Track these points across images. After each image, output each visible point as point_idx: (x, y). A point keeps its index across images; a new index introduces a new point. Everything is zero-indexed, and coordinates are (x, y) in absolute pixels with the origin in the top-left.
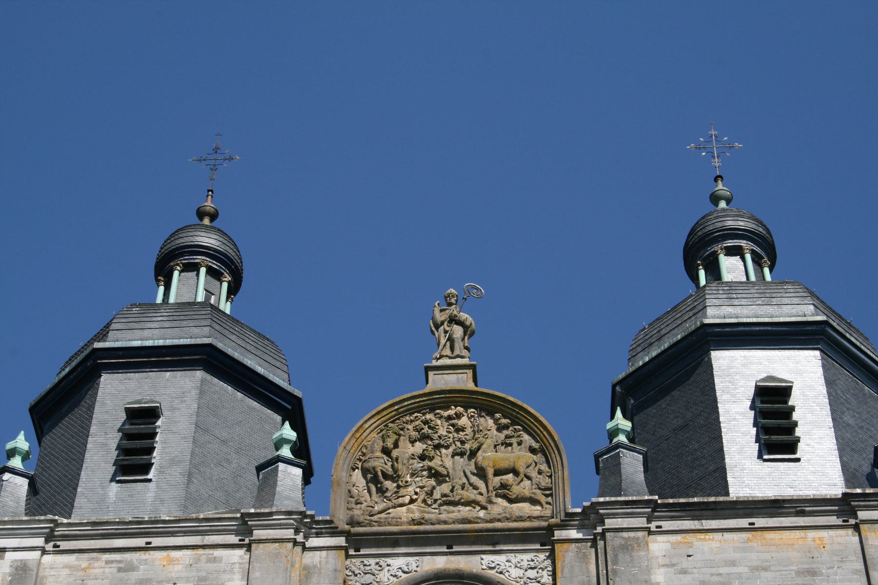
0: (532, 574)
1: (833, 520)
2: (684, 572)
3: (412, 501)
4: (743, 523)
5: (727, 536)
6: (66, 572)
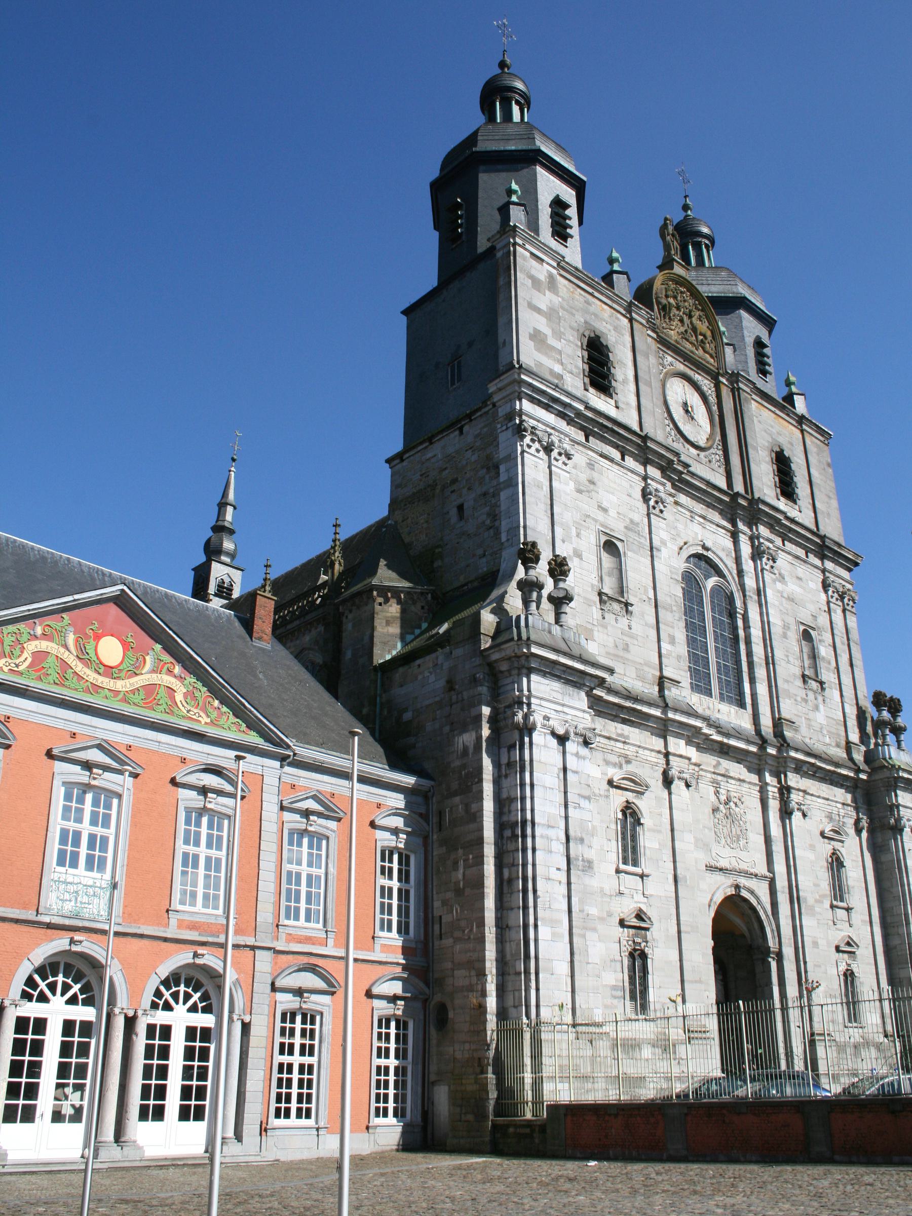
1: (794, 423)
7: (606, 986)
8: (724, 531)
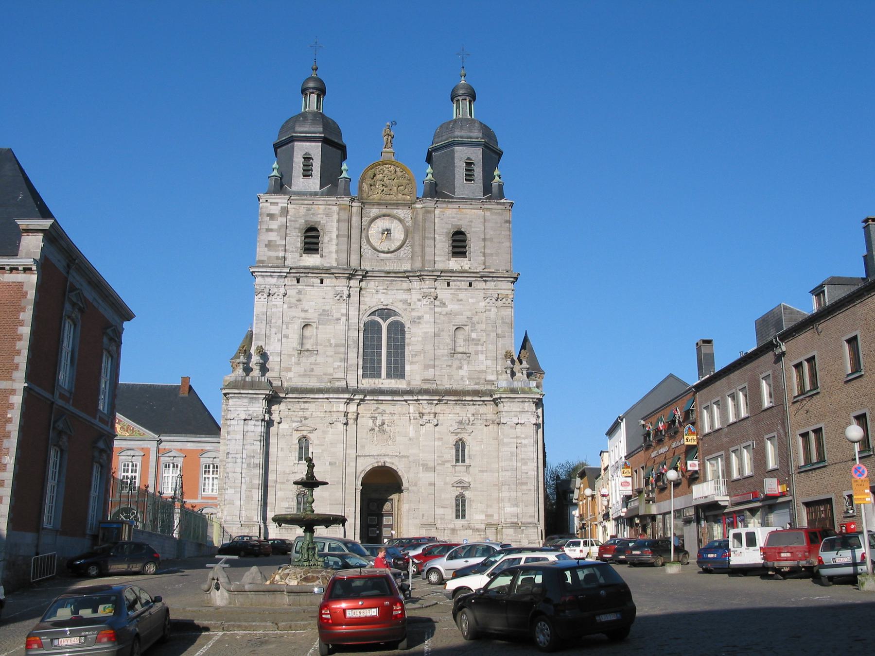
0: (406, 216)
2: (442, 219)
3: (378, 193)
5: (453, 210)
6: (294, 210)
7: (283, 507)
8: (402, 291)
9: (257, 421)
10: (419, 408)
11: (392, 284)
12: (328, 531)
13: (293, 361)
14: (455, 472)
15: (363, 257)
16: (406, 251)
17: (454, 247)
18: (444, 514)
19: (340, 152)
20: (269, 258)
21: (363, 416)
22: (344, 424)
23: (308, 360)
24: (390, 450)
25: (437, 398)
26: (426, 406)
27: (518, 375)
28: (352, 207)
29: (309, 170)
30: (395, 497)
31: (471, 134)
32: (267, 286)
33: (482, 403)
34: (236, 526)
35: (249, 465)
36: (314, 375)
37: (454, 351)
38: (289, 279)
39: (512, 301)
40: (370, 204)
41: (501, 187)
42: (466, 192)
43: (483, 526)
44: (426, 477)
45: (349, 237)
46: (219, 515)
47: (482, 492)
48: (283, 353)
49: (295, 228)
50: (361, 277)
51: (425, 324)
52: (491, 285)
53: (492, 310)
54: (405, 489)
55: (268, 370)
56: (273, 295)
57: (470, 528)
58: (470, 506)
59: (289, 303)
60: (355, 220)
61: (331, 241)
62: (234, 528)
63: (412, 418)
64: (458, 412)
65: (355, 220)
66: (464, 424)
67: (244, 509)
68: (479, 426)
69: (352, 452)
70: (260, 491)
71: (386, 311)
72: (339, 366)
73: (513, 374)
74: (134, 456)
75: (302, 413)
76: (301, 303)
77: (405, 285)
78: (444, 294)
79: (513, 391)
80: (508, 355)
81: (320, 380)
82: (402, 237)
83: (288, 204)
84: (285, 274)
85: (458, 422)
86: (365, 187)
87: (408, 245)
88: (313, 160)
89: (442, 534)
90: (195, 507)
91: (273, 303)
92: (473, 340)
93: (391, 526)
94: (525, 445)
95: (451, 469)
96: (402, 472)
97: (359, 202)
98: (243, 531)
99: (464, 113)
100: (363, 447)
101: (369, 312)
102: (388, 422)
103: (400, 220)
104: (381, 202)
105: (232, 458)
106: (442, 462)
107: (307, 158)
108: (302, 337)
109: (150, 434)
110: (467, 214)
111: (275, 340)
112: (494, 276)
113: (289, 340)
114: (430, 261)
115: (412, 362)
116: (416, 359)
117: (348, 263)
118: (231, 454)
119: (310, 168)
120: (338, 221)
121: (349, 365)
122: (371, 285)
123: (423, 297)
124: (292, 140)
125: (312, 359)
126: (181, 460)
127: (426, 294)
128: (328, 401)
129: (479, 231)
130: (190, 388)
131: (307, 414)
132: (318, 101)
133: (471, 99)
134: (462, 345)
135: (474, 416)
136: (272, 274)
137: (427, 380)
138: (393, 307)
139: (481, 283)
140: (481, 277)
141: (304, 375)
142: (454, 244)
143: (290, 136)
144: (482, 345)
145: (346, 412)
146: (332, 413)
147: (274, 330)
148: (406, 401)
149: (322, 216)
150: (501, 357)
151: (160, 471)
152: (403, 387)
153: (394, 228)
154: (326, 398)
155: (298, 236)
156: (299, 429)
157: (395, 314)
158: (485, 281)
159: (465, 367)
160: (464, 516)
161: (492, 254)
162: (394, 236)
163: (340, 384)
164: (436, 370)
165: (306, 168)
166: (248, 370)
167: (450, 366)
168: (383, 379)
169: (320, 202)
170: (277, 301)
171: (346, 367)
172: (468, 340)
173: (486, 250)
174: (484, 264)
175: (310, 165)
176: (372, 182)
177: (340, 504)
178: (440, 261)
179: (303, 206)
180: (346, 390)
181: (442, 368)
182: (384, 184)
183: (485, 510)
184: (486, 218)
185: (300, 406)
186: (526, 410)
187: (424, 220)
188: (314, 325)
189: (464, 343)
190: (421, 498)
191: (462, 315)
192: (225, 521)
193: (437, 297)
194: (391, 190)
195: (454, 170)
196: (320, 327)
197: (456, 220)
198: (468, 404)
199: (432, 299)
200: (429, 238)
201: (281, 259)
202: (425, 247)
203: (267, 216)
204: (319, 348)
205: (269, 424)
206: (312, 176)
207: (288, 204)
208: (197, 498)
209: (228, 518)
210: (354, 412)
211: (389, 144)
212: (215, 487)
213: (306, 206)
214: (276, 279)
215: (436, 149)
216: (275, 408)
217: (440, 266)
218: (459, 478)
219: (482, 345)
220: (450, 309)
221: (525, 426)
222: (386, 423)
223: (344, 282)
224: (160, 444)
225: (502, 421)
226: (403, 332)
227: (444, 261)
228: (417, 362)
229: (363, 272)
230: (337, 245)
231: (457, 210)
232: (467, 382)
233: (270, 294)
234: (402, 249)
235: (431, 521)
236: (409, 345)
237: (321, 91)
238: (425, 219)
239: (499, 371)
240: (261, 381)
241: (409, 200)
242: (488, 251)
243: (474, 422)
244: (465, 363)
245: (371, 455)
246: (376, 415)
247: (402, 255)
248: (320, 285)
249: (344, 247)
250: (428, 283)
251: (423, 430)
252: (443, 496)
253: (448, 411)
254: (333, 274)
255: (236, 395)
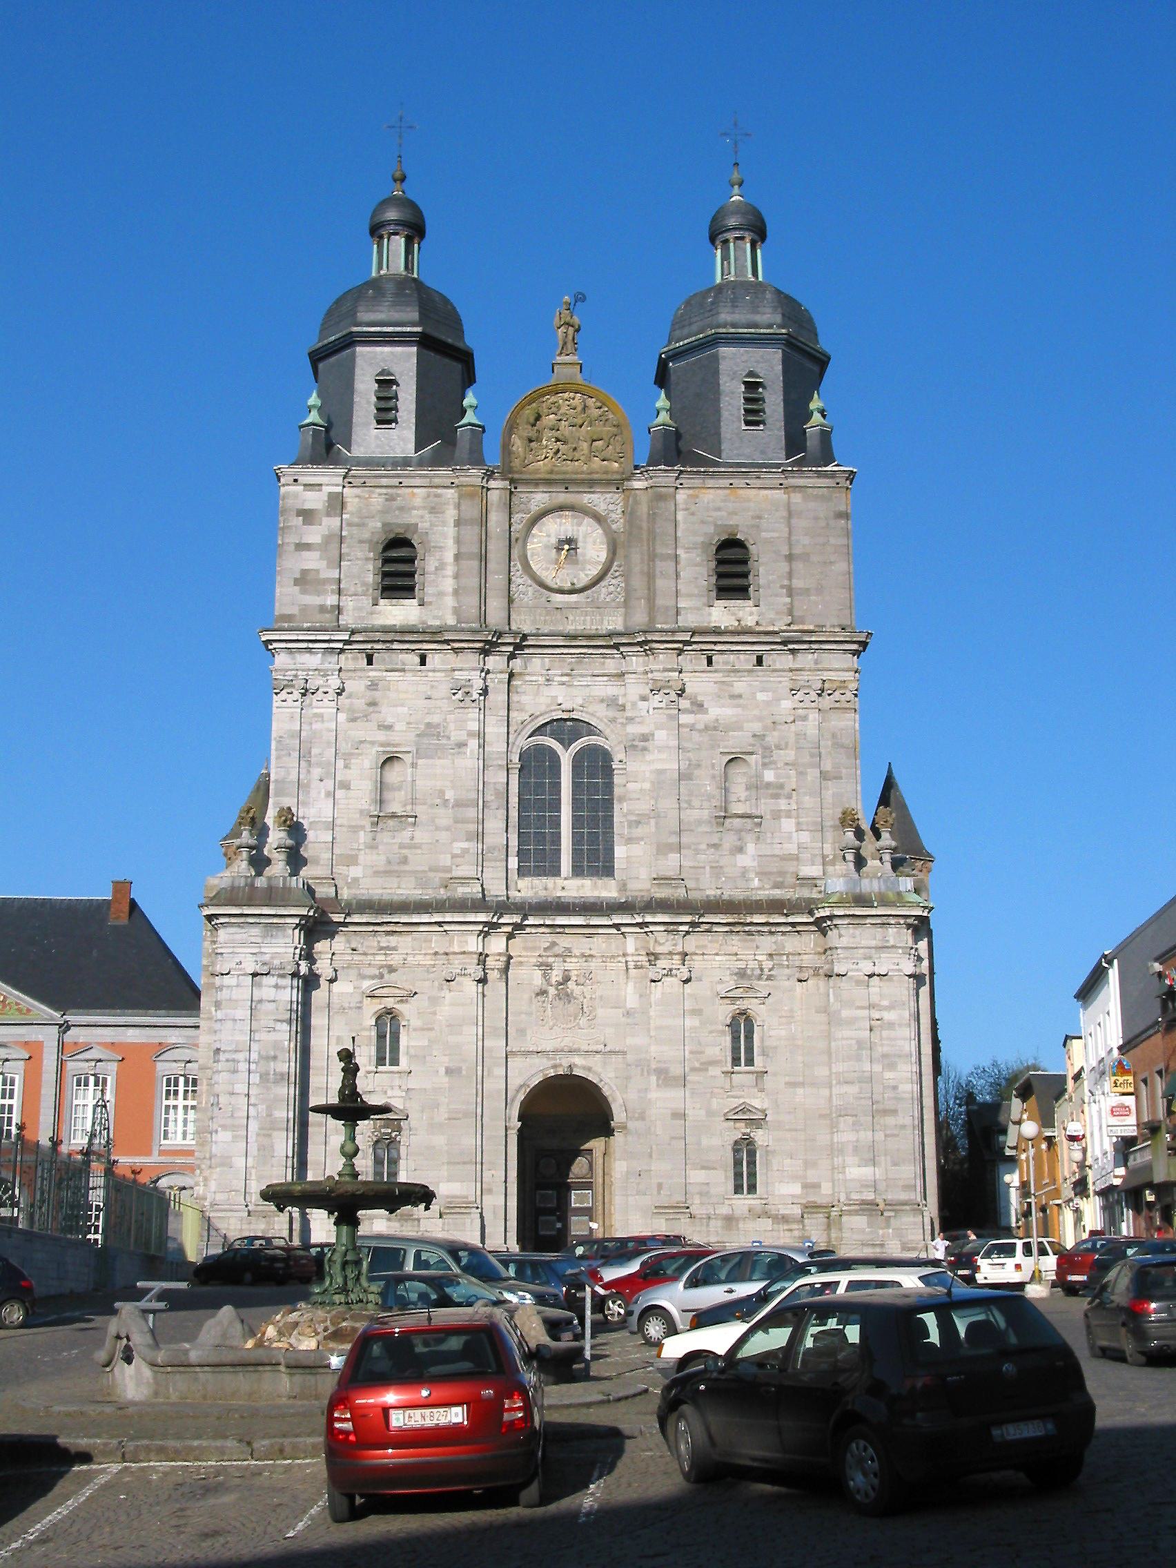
0: (611, 507)
2: (693, 514)
3: (546, 458)
4: (726, 483)
6: (357, 500)
8: (605, 678)
9: (282, 976)
10: (648, 942)
11: (581, 662)
12: (444, 1224)
13: (362, 841)
14: (732, 1087)
15: (515, 605)
16: (612, 588)
17: (720, 576)
18: (708, 1184)
19: (458, 366)
20: (304, 609)
21: (521, 963)
22: (479, 981)
23: (394, 837)
24: (582, 1038)
25: (688, 919)
26: (662, 937)
27: (872, 863)
28: (488, 489)
29: (390, 409)
30: (596, 1144)
31: (758, 318)
32: (300, 673)
33: (789, 928)
34: (236, 1214)
35: (264, 1077)
36: (409, 872)
37: (726, 812)
38: (350, 656)
39: (856, 695)
40: (527, 482)
41: (825, 436)
42: (747, 451)
43: (797, 1211)
44: (663, 1100)
45: (483, 558)
46: (200, 1190)
47: (793, 1133)
48: (338, 822)
49: (361, 542)
50: (511, 649)
51: (659, 751)
52: (806, 660)
53: (811, 717)
54: (619, 1128)
55: (304, 862)
56: (313, 693)
57: (766, 1214)
58: (767, 1164)
59: (349, 710)
60: (496, 519)
61: (443, 569)
62: (232, 1221)
63: (631, 965)
64: (735, 950)
65: (496, 519)
66: (750, 978)
67: (253, 1177)
68: (785, 980)
69: (496, 1044)
70: (291, 1135)
71: (568, 723)
72: (465, 851)
73: (860, 862)
74: (7, 1060)
75: (383, 958)
76: (377, 709)
77: (612, 665)
78: (700, 683)
79: (861, 900)
80: (848, 819)
81: (423, 883)
82: (603, 556)
83: (344, 487)
84: (340, 645)
85: (736, 974)
86: (518, 444)
87: (617, 574)
88: (398, 385)
89: (704, 1228)
90: (139, 1173)
91: (316, 711)
92: (768, 785)
93: (589, 1213)
94: (891, 1025)
95: (723, 1081)
96: (611, 1088)
97: (502, 480)
98: (252, 1227)
99: (740, 270)
100: (522, 1032)
101: (529, 726)
102: (577, 976)
103: (598, 518)
104: (554, 477)
105: (227, 1060)
106: (702, 1064)
107: (386, 383)
108: (382, 787)
109: (39, 1009)
110: (749, 500)
111: (319, 793)
112: (813, 639)
113: (351, 793)
114: (667, 608)
115: (630, 839)
116: (639, 831)
117: (482, 617)
118: (224, 1052)
119: (391, 404)
120: (458, 523)
121: (488, 848)
122: (534, 665)
123: (652, 691)
124: (349, 342)
125: (406, 835)
126: (113, 1067)
127: (659, 684)
128: (441, 929)
129: (778, 538)
130: (133, 905)
131: (395, 959)
132: (408, 251)
133: (756, 237)
134: (742, 799)
135: (772, 960)
136: (311, 645)
137: (667, 879)
138: (584, 715)
139: (783, 656)
140: (784, 643)
141: (385, 872)
142: (723, 569)
143: (344, 333)
144: (789, 797)
145: (481, 954)
146: (451, 957)
147: (317, 772)
148: (617, 926)
149: (420, 512)
150: (831, 823)
151: (67, 1094)
152: (610, 895)
153: (585, 537)
154: (436, 923)
155: (367, 559)
156: (377, 993)
157: (590, 730)
158: (793, 651)
159: (751, 848)
160: (752, 1188)
161: (808, 589)
162: (584, 555)
163: (468, 890)
164: (685, 856)
165: (383, 405)
166: (259, 862)
167: (716, 846)
168: (566, 879)
169: (418, 482)
170: (323, 706)
171: (480, 851)
172: (757, 786)
173: (794, 581)
174: (790, 613)
175: (391, 398)
176: (533, 434)
177: (470, 1163)
178: (691, 608)
179: (378, 490)
180: (480, 904)
181: (697, 851)
182: (561, 437)
183: (801, 1173)
184: (793, 508)
185: (379, 942)
186: (892, 943)
187: (652, 517)
188: (408, 758)
189: (747, 793)
190: (654, 1147)
191: (740, 729)
192: (212, 1205)
193: (683, 690)
194: (575, 449)
195: (717, 400)
196: (420, 762)
197: (724, 513)
198: (759, 931)
199: (673, 696)
200: (665, 558)
201: (331, 612)
202: (654, 577)
203: (298, 515)
204: (419, 810)
205: (309, 983)
206: (397, 423)
207: (344, 487)
208: (149, 1153)
209: (220, 1197)
210: (500, 954)
211: (570, 345)
212: (191, 1128)
213: (384, 491)
214: (320, 655)
215: (676, 355)
216: (319, 946)
217: (689, 619)
218: (742, 1101)
219: (789, 797)
220: (714, 717)
221: (891, 980)
222: (574, 978)
223: (473, 659)
224: (65, 1032)
225: (836, 970)
226: (608, 772)
227: (698, 609)
228: (642, 839)
229: (515, 638)
230: (456, 576)
231: (727, 491)
232: (756, 883)
233: (307, 690)
234: (603, 583)
235: (678, 1198)
236: (621, 800)
237: (415, 230)
238: (654, 513)
239: (828, 856)
240: (290, 888)
241: (617, 472)
242: (797, 583)
243: (771, 973)
244: (749, 837)
245: (539, 1050)
246: (551, 960)
247: (602, 596)
248: (419, 668)
249: (473, 582)
250: (664, 659)
251: (657, 991)
252: (705, 1142)
253: (712, 949)
254: (447, 642)
255: (233, 920)
